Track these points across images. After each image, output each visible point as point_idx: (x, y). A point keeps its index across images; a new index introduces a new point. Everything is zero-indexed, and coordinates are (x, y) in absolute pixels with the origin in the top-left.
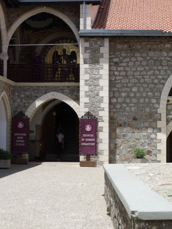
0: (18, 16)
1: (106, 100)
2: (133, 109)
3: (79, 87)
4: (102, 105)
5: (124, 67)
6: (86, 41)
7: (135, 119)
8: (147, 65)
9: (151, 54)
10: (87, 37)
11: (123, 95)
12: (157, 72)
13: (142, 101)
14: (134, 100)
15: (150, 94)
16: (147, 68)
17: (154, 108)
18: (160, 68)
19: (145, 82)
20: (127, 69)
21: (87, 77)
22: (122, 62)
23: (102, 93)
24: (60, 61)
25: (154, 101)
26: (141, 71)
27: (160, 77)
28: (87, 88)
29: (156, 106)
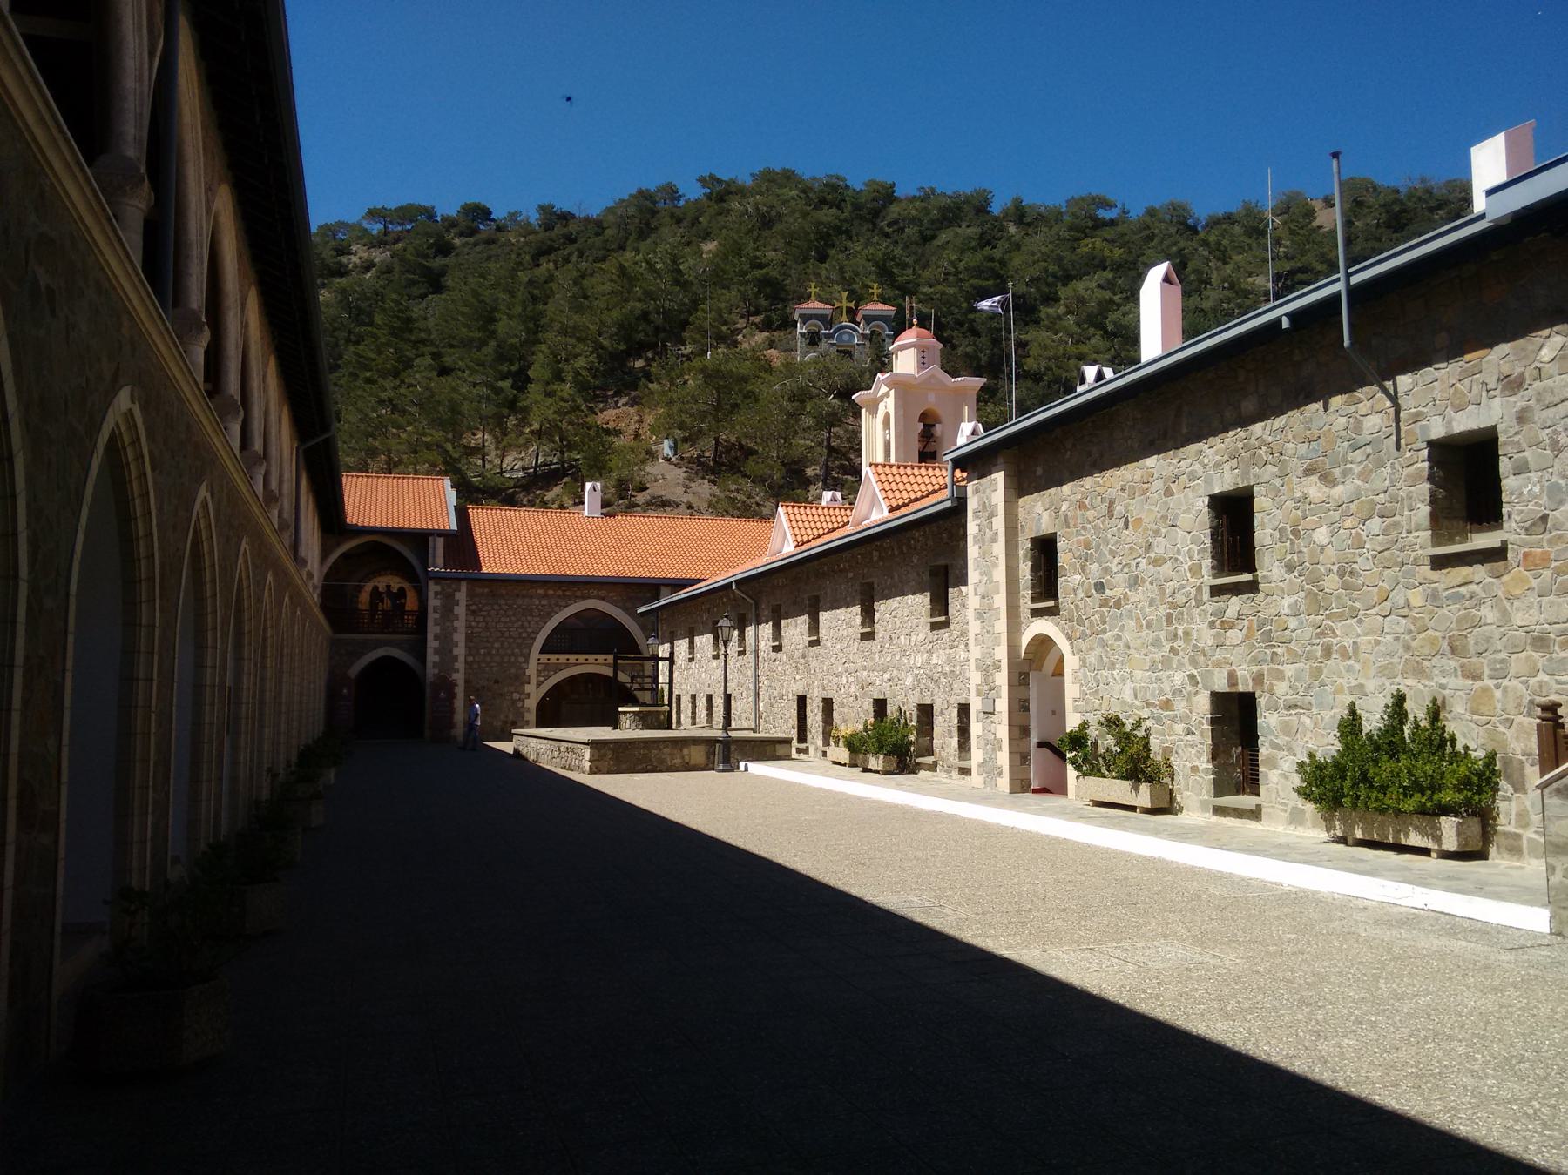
0: (338, 545)
1: (462, 659)
2: (495, 669)
3: (425, 641)
4: (457, 665)
5: (484, 617)
6: (436, 584)
7: (497, 682)
8: (514, 615)
9: (520, 601)
10: (438, 578)
11: (482, 651)
12: (526, 624)
13: (506, 660)
14: (497, 659)
15: (517, 650)
16: (513, 618)
17: (522, 668)
18: (530, 618)
19: (510, 637)
20: (488, 619)
21: (437, 629)
22: (481, 610)
23: (456, 651)
24: (383, 603)
25: (521, 660)
26: (506, 622)
27: (530, 630)
28: (436, 644)
29: (524, 665)
